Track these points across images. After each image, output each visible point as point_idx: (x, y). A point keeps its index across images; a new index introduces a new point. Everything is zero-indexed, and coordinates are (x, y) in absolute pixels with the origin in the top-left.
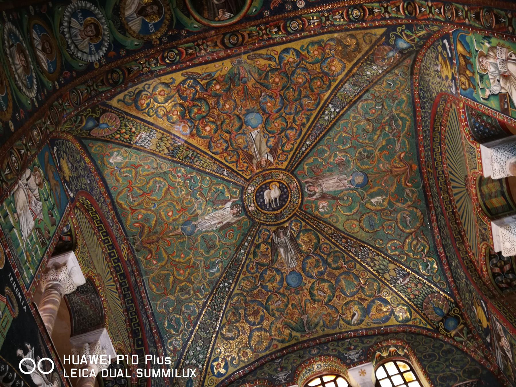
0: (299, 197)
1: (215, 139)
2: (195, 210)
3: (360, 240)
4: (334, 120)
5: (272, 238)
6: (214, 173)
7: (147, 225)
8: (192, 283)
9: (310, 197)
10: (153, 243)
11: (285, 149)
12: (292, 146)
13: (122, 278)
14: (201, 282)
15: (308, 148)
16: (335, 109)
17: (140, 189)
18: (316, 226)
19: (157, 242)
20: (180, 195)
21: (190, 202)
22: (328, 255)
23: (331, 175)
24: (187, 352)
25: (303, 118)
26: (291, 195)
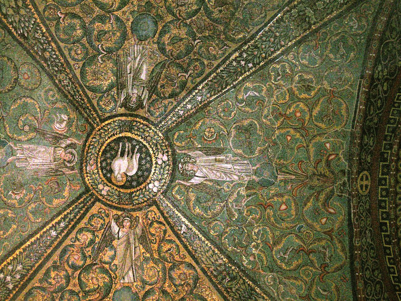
0: (89, 147)
1: (186, 288)
2: (248, 196)
3: (25, 49)
4: (8, 260)
5: (149, 99)
6: (200, 236)
7: (320, 204)
8: (290, 91)
9: (75, 144)
10: (321, 175)
11: (90, 236)
12: (79, 236)
13: (386, 155)
14: (278, 87)
15: (56, 223)
16: (5, 278)
17: (312, 262)
18: (78, 91)
19: (314, 174)
20: (261, 228)
21: (250, 212)
22: (78, 41)
23: (36, 172)
24: (346, 4)
25: (54, 279)
26: (98, 154)
